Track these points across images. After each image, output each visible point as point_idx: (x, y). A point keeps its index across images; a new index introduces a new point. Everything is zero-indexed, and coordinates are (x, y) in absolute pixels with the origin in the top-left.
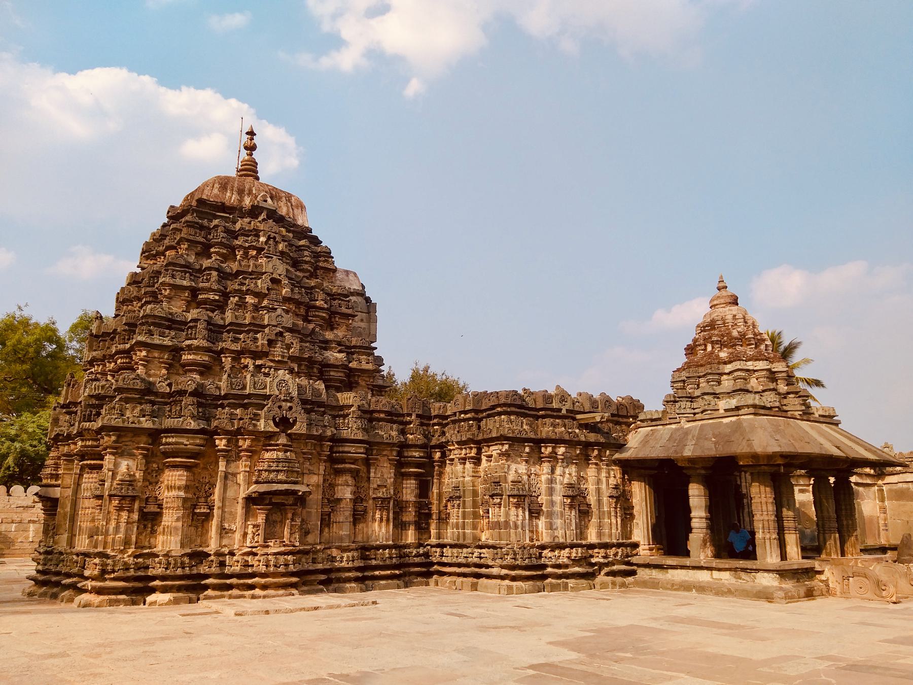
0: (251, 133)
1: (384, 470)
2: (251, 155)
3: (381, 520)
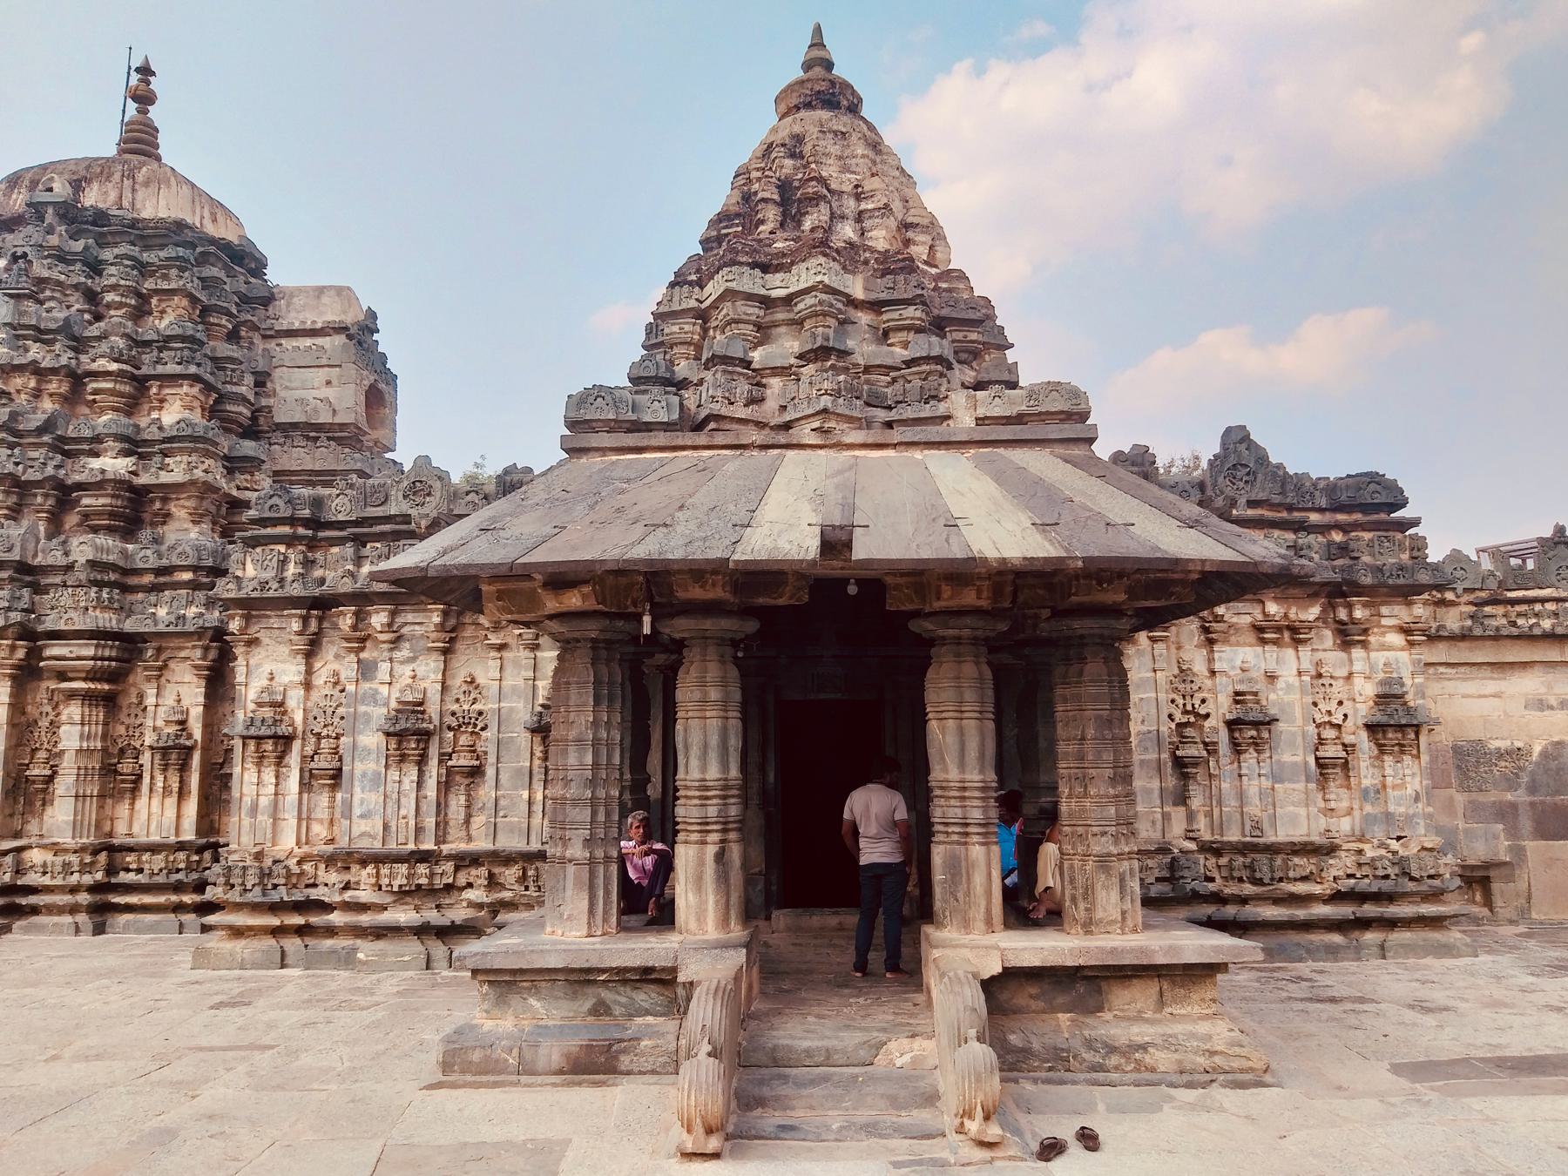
0: (146, 71)
1: (183, 690)
2: (144, 112)
3: (166, 790)
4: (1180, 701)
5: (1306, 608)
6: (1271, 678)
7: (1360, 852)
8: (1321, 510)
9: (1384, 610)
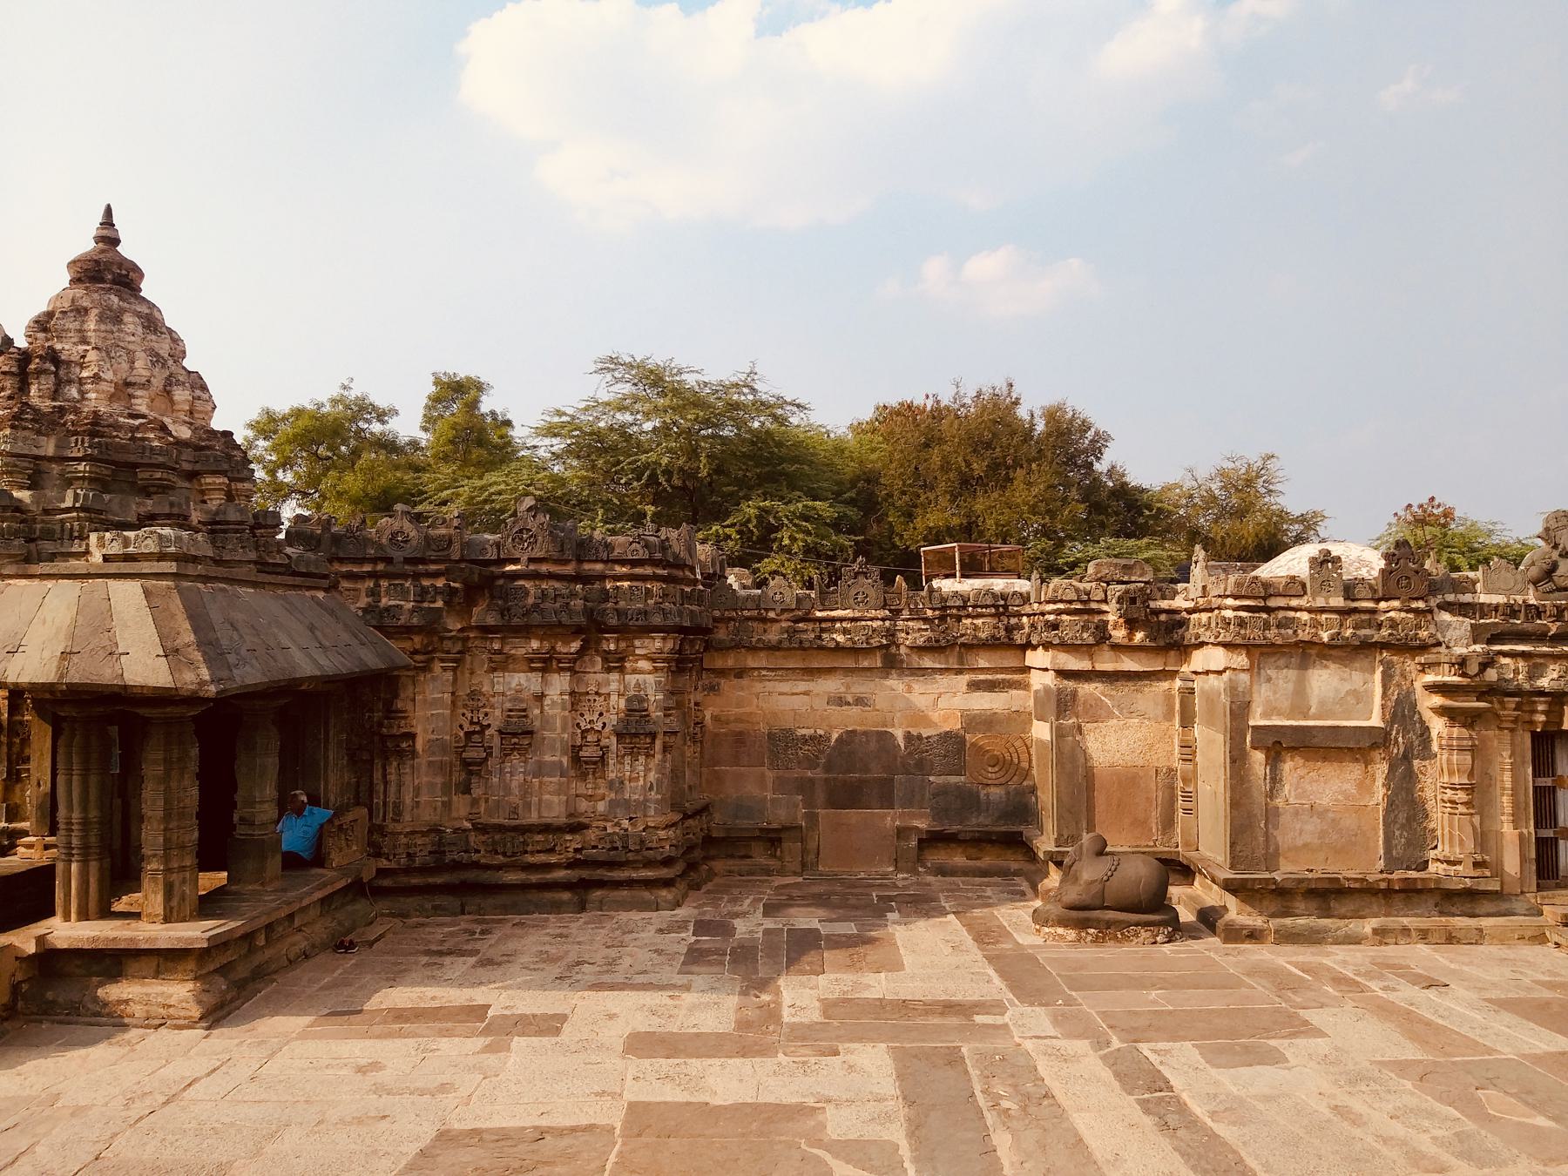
4: (469, 715)
5: (567, 643)
6: (540, 697)
7: (605, 829)
8: (602, 561)
9: (637, 643)
